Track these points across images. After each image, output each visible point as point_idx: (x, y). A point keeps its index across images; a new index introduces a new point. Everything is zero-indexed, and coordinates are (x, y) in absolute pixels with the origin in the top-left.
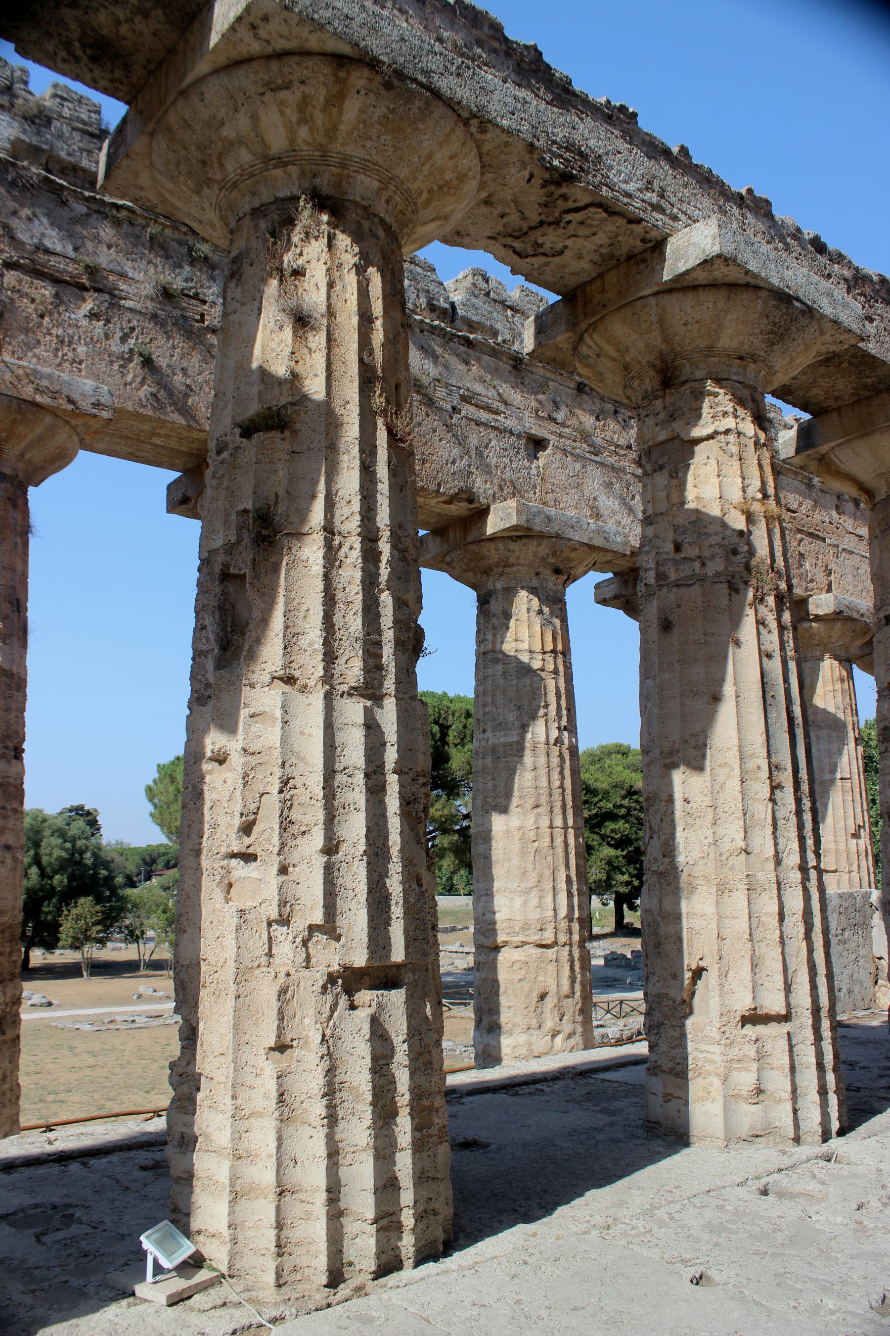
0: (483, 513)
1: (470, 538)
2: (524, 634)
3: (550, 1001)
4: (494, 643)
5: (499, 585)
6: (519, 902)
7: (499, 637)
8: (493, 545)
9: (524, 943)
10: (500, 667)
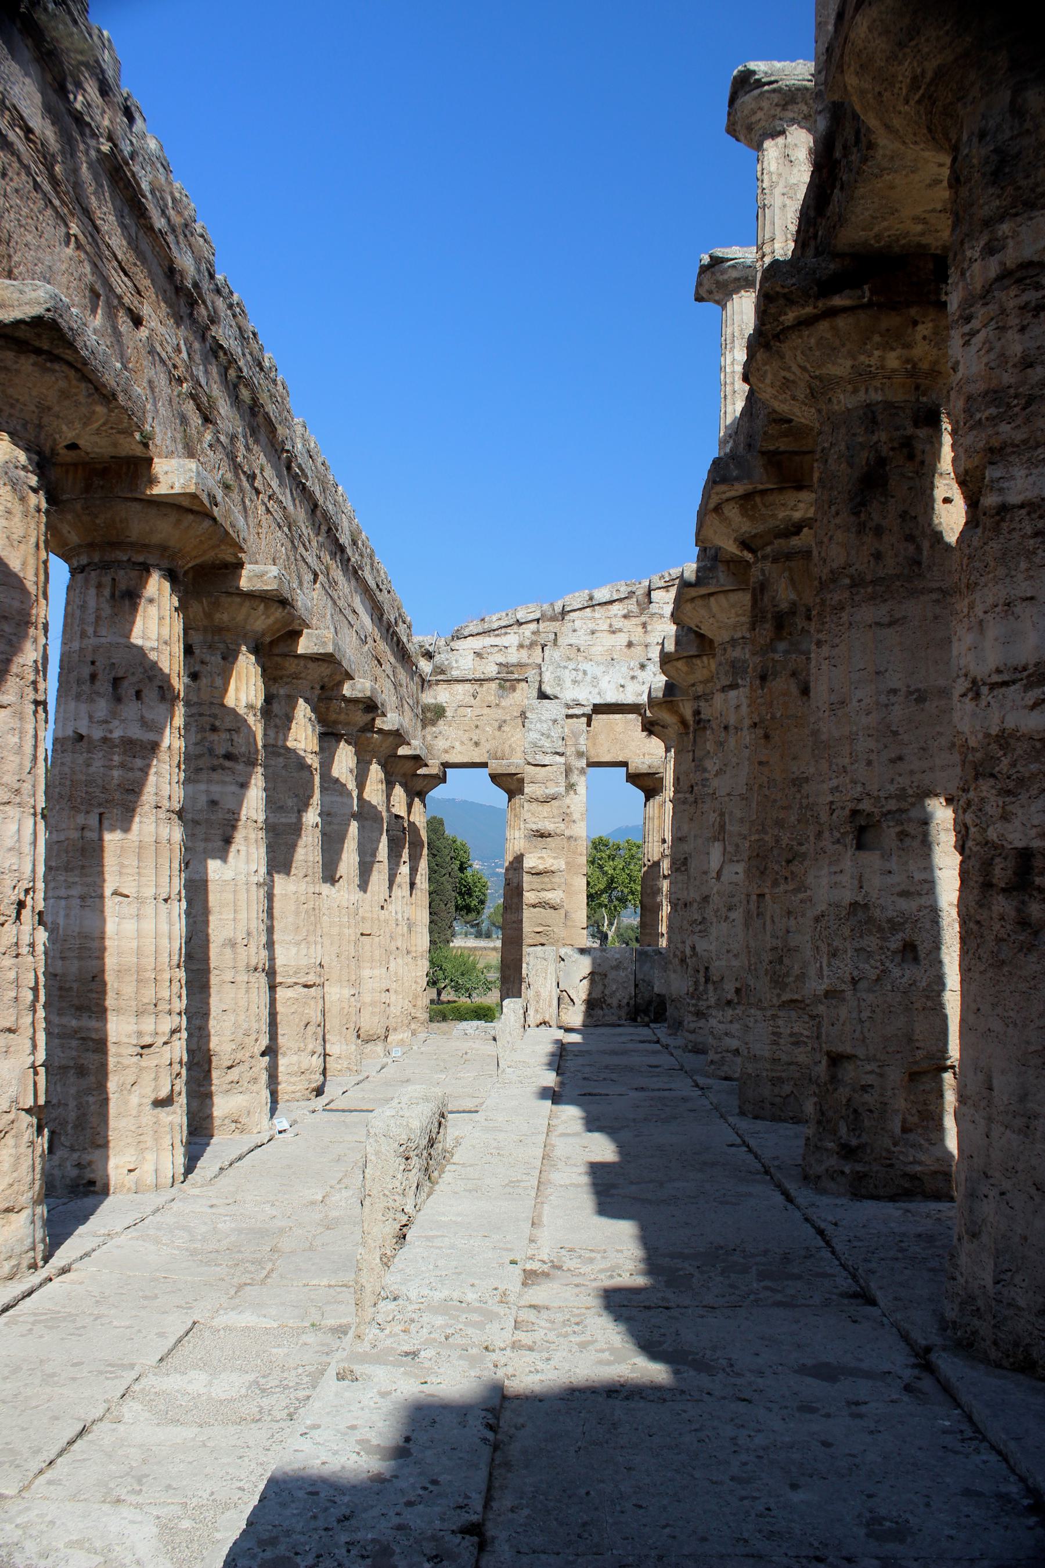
0: (299, 634)
1: (276, 651)
2: (302, 736)
3: (311, 1029)
4: (276, 739)
5: (282, 692)
6: (294, 950)
7: (281, 736)
8: (296, 661)
9: (296, 984)
10: (281, 760)
